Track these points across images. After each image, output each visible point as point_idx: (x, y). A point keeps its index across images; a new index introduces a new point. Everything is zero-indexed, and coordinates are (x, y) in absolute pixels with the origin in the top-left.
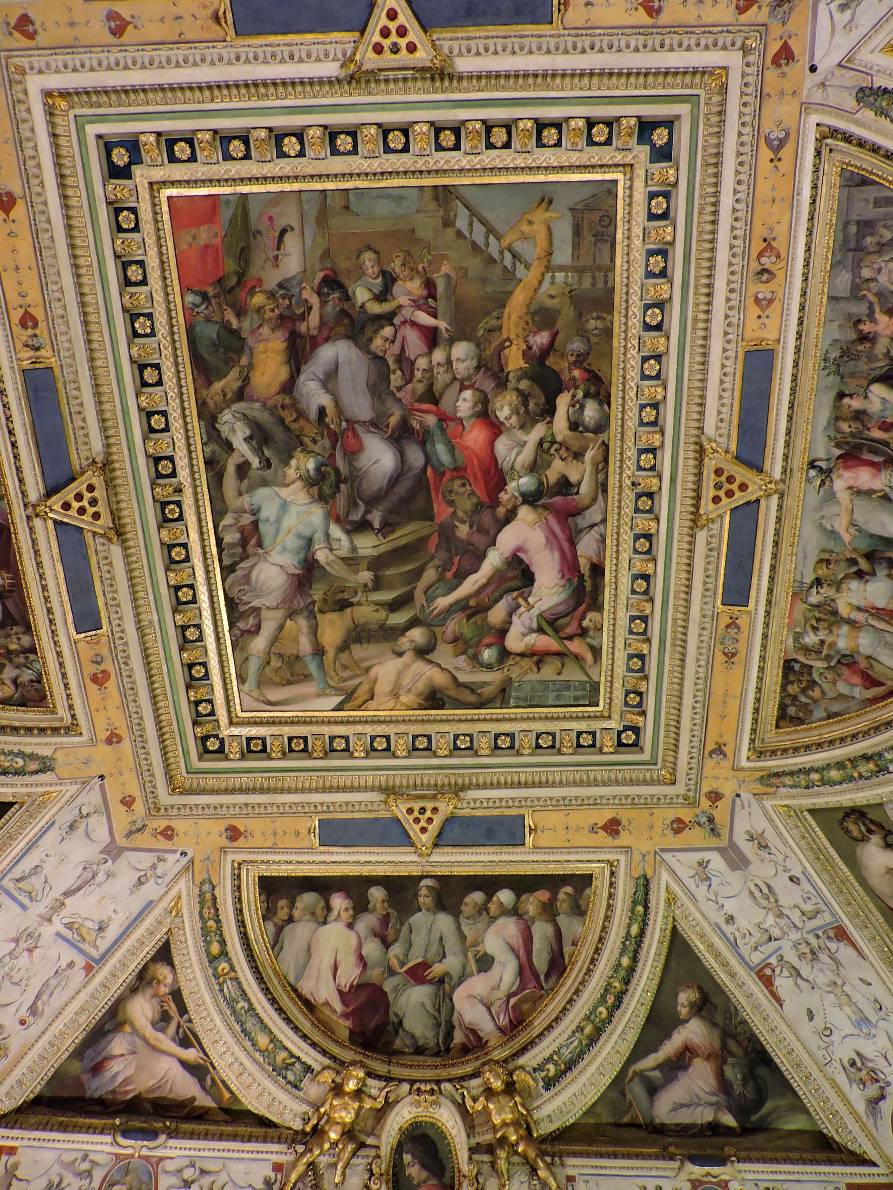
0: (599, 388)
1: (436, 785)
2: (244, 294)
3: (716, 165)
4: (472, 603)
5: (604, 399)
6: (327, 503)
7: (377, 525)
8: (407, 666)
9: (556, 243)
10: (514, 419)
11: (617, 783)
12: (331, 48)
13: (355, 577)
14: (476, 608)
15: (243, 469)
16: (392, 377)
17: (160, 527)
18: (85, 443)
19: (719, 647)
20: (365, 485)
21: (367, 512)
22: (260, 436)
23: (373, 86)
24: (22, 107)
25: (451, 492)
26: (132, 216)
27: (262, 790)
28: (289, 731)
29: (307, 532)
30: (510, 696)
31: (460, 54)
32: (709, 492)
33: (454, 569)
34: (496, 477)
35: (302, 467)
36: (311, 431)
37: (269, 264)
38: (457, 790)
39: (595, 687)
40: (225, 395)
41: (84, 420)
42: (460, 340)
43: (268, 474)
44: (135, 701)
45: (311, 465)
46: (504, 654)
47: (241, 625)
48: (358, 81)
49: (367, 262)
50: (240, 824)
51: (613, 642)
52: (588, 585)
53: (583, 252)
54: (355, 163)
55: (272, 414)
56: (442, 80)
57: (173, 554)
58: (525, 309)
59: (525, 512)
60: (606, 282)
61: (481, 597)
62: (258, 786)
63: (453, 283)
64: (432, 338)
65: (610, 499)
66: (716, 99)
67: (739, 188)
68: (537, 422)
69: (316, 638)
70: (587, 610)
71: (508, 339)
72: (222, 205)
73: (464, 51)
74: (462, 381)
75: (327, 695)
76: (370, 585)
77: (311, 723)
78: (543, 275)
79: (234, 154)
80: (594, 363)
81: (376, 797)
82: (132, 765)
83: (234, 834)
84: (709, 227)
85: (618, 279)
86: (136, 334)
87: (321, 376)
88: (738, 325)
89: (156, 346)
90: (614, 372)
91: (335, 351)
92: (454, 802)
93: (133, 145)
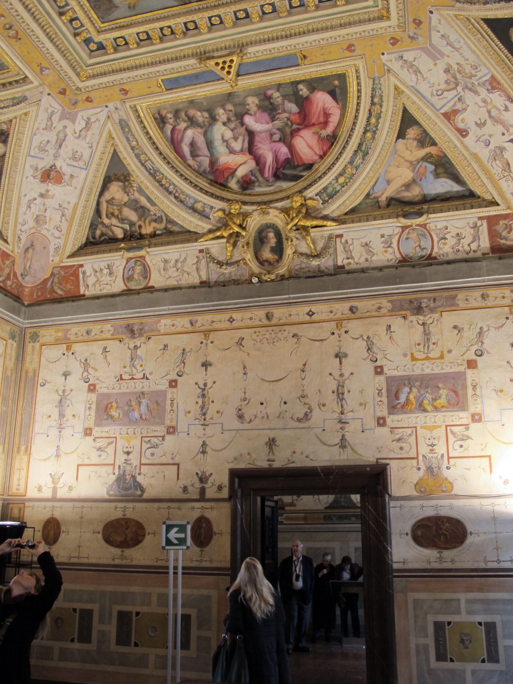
24: (401, 15)
31: (196, 64)
48: (238, 45)
56: (201, 53)
66: (79, 70)
84: (48, 30)
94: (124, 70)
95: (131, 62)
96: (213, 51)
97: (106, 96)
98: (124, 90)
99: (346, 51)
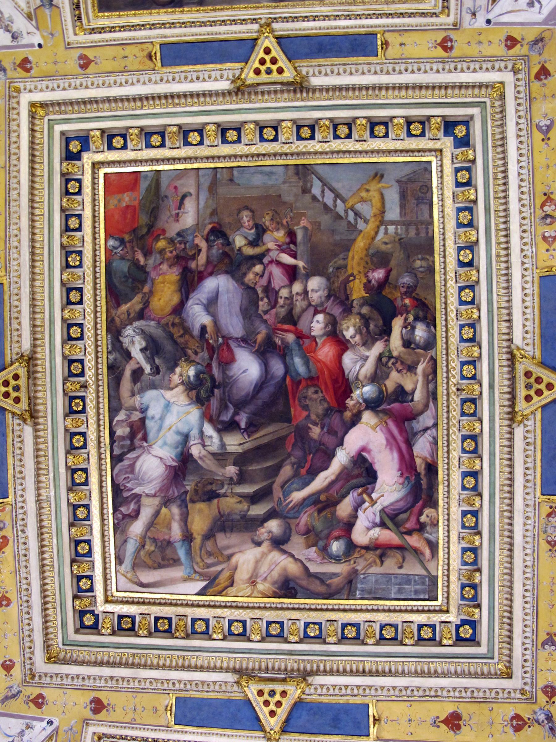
0: (426, 313)
1: (286, 670)
2: (150, 240)
3: (502, 145)
4: (323, 497)
5: (431, 322)
6: (202, 404)
7: (243, 425)
8: (264, 555)
9: (388, 205)
10: (358, 338)
11: (457, 675)
12: (225, 74)
13: (223, 470)
14: (325, 503)
15: (137, 374)
16: (261, 303)
17: (66, 416)
18: (18, 342)
19: (543, 536)
20: (235, 390)
21: (236, 413)
22: (153, 348)
23: (253, 97)
24: (15, 112)
25: (305, 397)
26: (77, 184)
27: (127, 665)
28: (156, 611)
29: (185, 430)
30: (356, 588)
31: (314, 75)
32: (521, 392)
33: (307, 466)
34: (342, 386)
35: (184, 374)
36: (194, 345)
37: (172, 219)
38: (304, 675)
39: (434, 580)
40: (129, 315)
41: (19, 324)
42: (314, 275)
43: (158, 380)
44: (26, 567)
45: (192, 372)
46: (351, 547)
47: (123, 509)
48: (243, 94)
49: (245, 218)
50: (103, 697)
51: (448, 536)
52: (424, 482)
53: (408, 211)
54: (239, 149)
55: (165, 331)
56: (301, 92)
57: (74, 440)
58: (365, 252)
59: (368, 417)
60: (427, 233)
61: (331, 492)
62: (124, 661)
63: (309, 233)
64: (292, 273)
65: (439, 405)
66: (498, 103)
67: (521, 159)
68: (377, 340)
69: (186, 525)
70: (424, 507)
71: (352, 275)
72: (142, 179)
73: (317, 73)
74: (315, 307)
75: (193, 580)
76: (235, 479)
77: (176, 605)
78: (378, 227)
79: (154, 144)
80: (420, 292)
81: (230, 677)
82: (16, 630)
83: (98, 706)
84: (502, 188)
85: (436, 230)
86: (68, 266)
87: (205, 302)
88: (532, 257)
89: (81, 274)
90: (438, 300)
91: (217, 283)
92: (303, 685)
93: (84, 140)
94: (427, 87)
95: (413, 97)
96: (282, 92)
97: (480, 42)
98: (446, 49)
99: (92, 58)
